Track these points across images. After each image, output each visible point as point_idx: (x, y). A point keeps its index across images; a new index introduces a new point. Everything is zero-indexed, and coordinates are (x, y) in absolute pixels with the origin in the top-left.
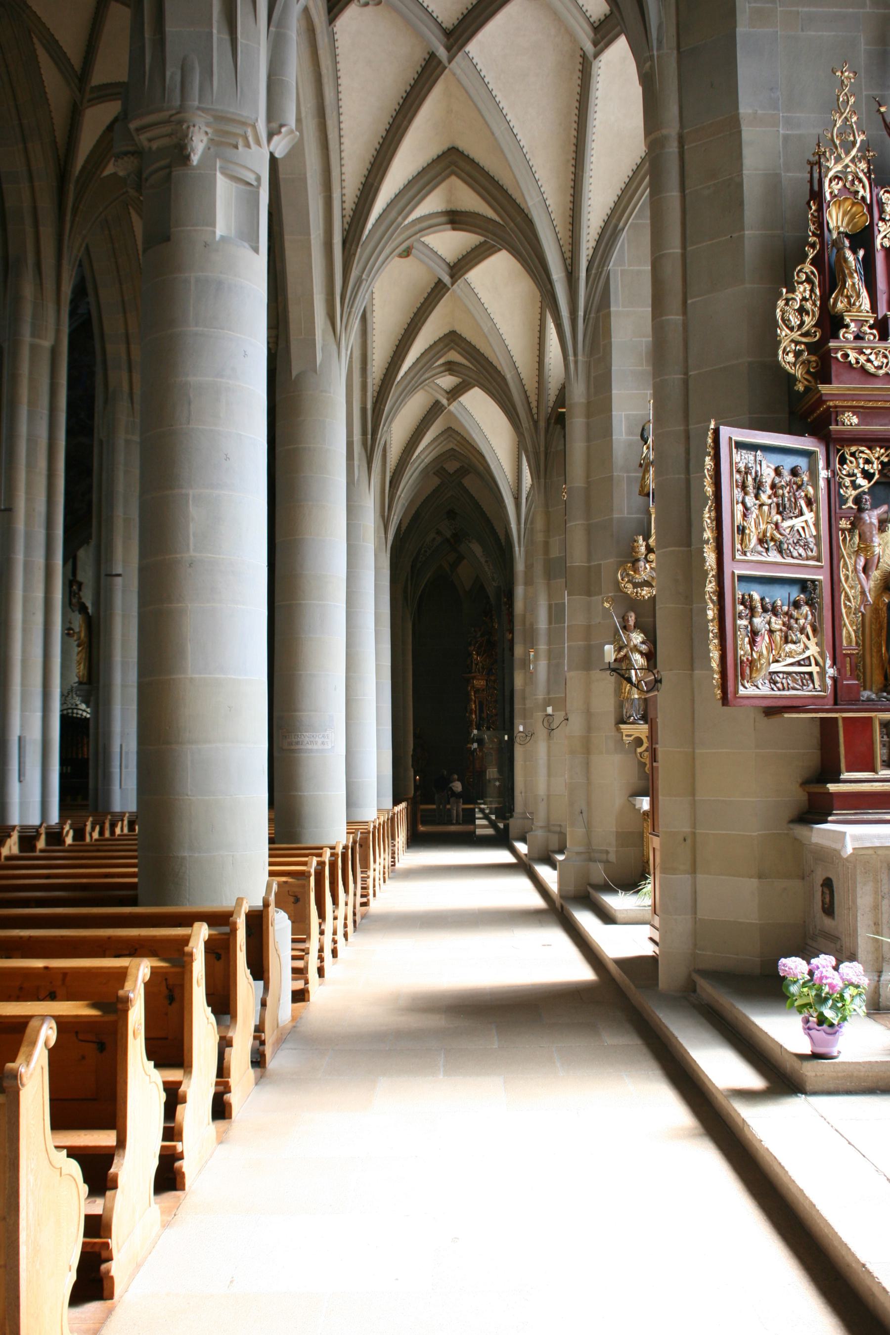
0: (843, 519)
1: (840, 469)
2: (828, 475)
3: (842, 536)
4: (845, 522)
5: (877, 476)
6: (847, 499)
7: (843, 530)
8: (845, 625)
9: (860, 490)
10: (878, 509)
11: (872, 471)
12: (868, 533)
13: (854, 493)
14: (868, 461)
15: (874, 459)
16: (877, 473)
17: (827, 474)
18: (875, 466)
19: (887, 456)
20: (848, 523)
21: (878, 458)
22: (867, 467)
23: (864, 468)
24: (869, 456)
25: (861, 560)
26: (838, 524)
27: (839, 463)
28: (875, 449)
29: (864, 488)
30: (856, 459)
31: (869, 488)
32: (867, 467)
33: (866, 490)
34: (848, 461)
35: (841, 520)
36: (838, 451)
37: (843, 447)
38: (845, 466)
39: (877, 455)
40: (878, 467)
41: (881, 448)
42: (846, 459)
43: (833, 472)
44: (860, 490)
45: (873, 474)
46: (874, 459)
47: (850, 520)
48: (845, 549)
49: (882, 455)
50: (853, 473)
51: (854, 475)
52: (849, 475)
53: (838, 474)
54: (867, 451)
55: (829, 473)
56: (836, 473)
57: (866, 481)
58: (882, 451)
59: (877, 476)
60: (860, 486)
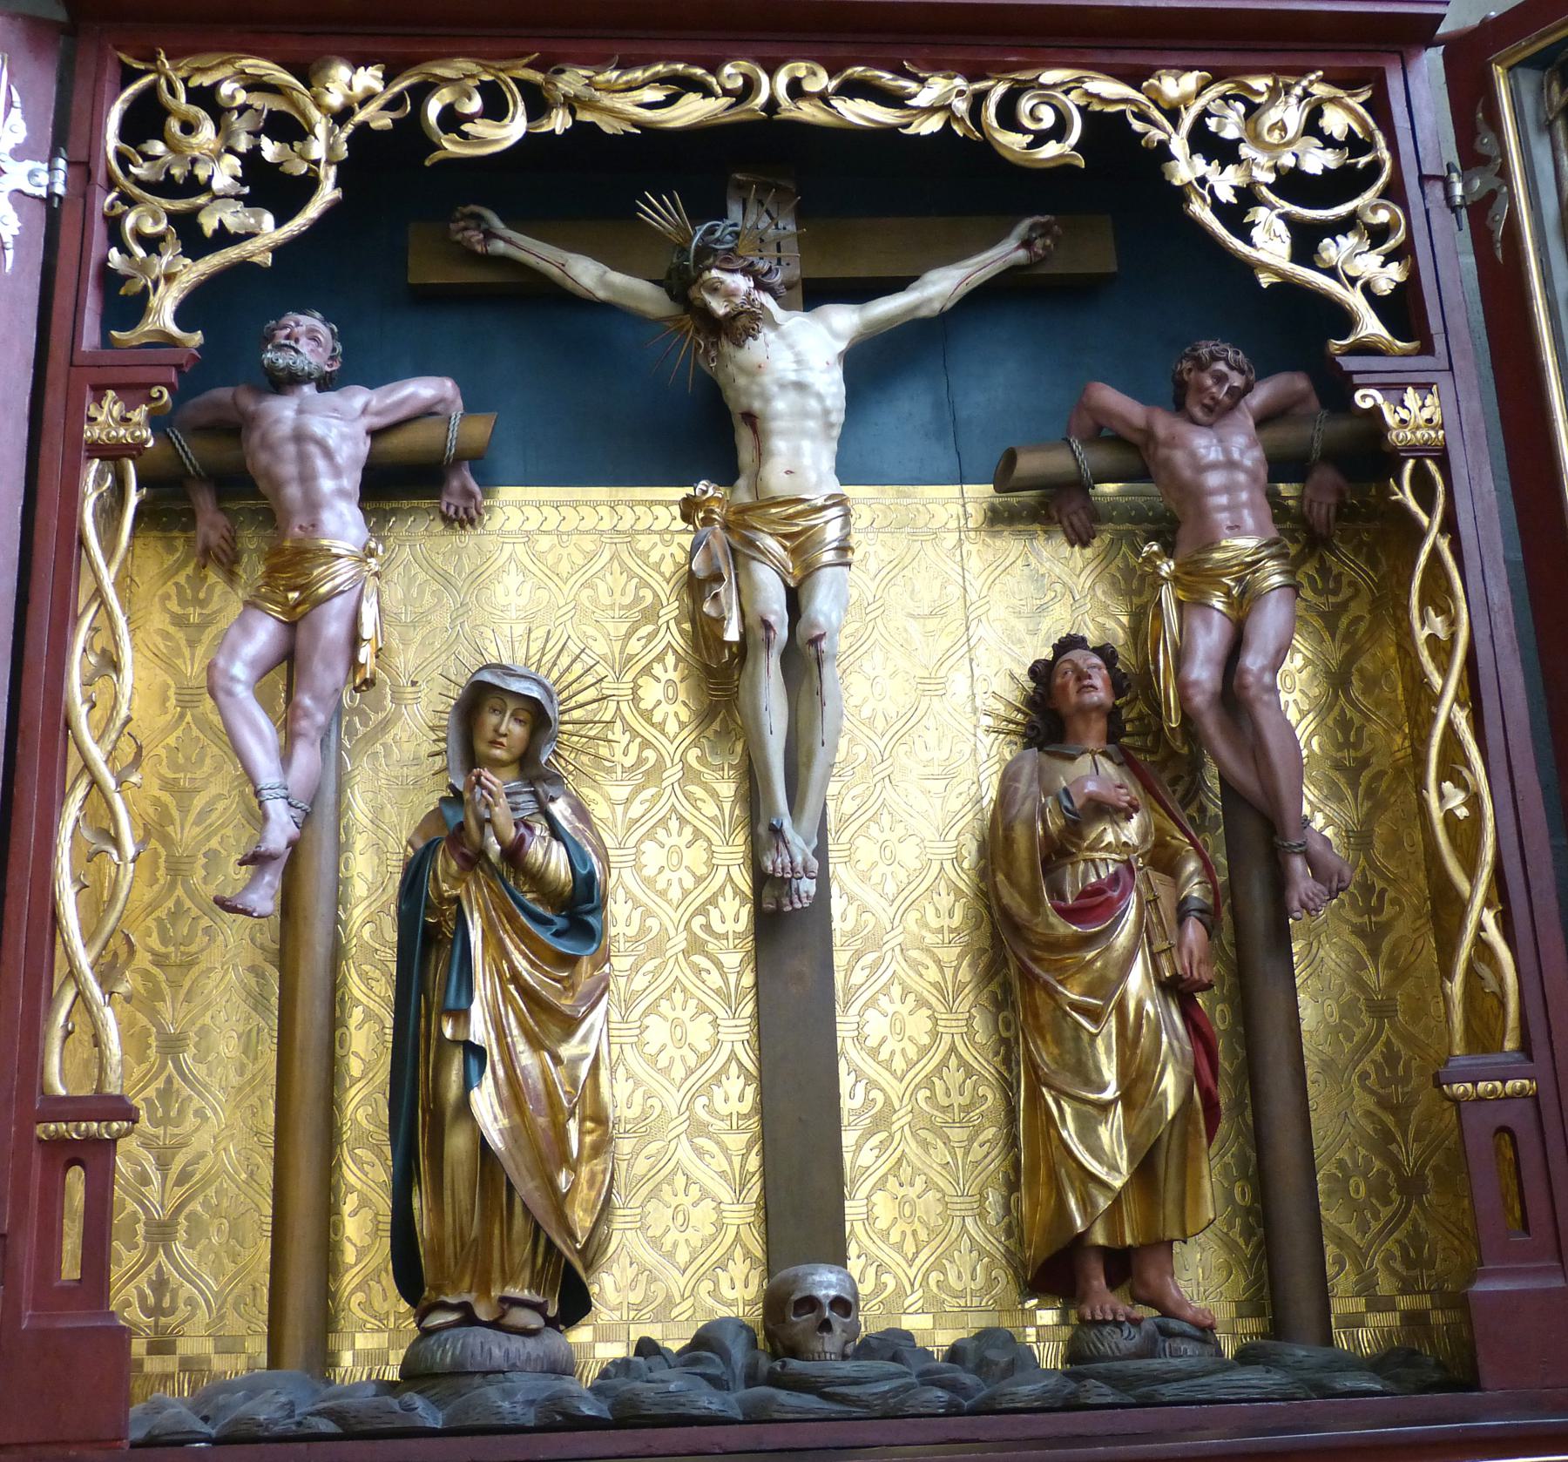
0: (111, 394)
1: (123, 160)
2: (51, 184)
3: (98, 482)
4: (116, 410)
5: (328, 193)
6: (144, 295)
7: (112, 454)
8: (73, 974)
9: (232, 254)
10: (385, 388)
11: (302, 168)
12: (293, 492)
13: (193, 272)
14: (289, 129)
15: (316, 115)
16: (329, 176)
17: (44, 178)
18: (318, 150)
19: (390, 106)
20: (139, 414)
21: (341, 116)
22: (270, 150)
23: (257, 149)
24: (294, 103)
25: (247, 632)
26: (76, 417)
27: (123, 136)
28: (326, 65)
29: (248, 247)
30: (218, 112)
31: (278, 251)
32: (270, 150)
33: (268, 259)
34: (174, 125)
35: (98, 401)
36: (129, 76)
37: (152, 58)
38: (158, 148)
39: (335, 99)
40: (331, 148)
41: (358, 61)
42: (166, 113)
43: (83, 169)
44: (232, 254)
45: (309, 184)
46: (321, 125)
47: (150, 400)
48: (109, 552)
49: (369, 97)
50: (192, 177)
51: (195, 186)
52: (166, 187)
53: (111, 183)
54: (285, 77)
55: (60, 177)
56: (100, 176)
57: (268, 219)
58: (369, 78)
59: (328, 193)
60: (224, 238)
